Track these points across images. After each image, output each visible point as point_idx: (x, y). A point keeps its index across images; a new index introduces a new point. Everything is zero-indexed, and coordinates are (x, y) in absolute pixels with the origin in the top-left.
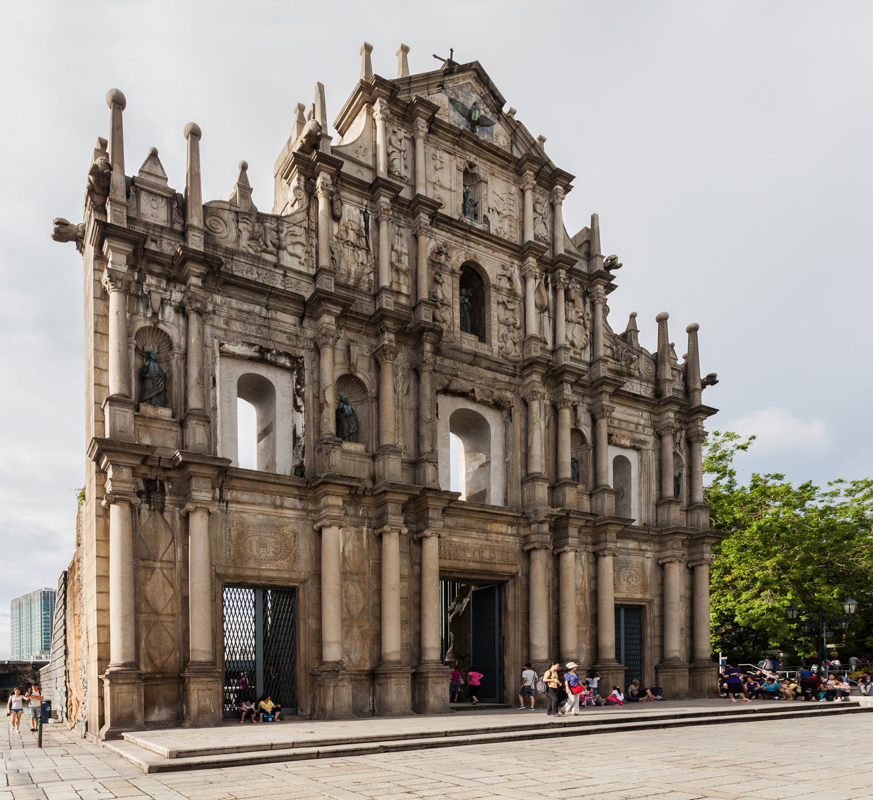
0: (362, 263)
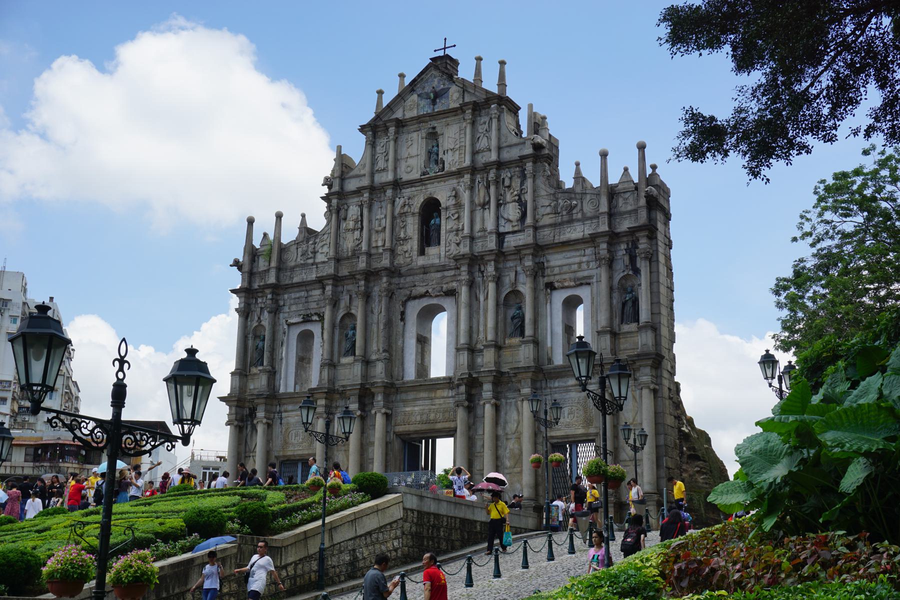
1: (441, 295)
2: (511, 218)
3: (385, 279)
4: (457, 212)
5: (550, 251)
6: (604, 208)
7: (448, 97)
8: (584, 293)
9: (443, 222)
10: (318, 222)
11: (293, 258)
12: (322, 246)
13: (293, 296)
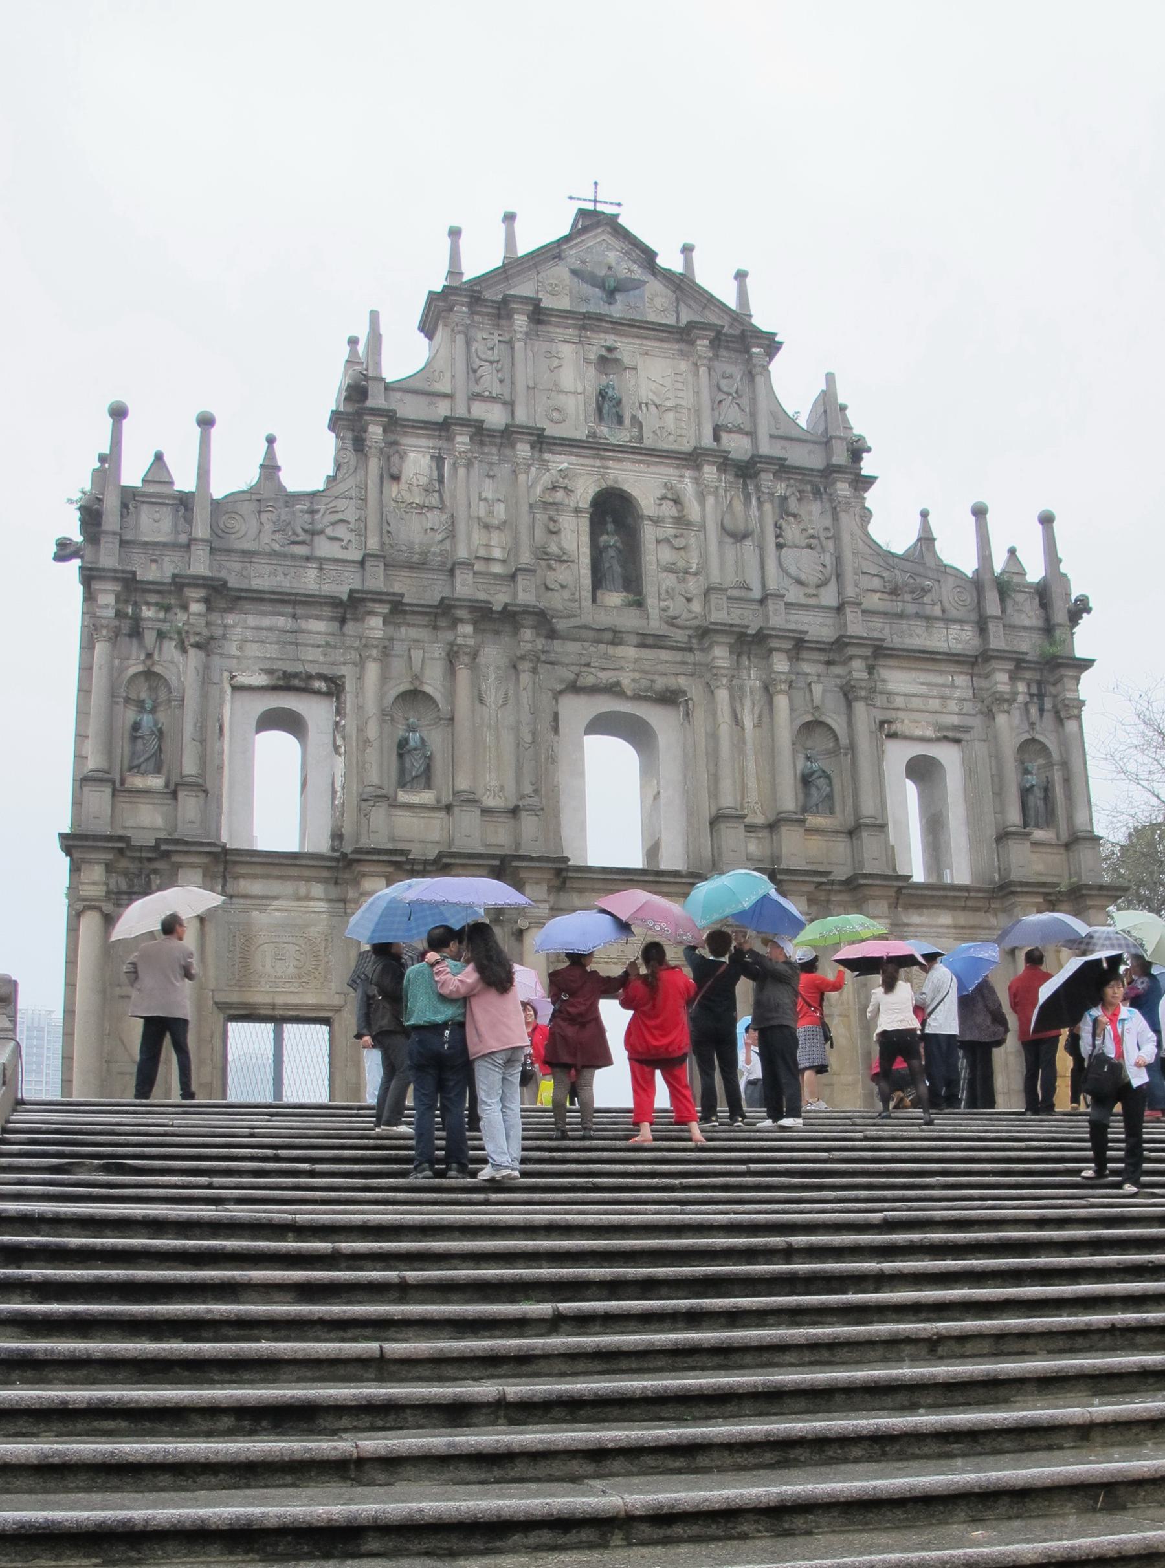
0: (432, 529)
1: (646, 699)
2: (803, 577)
4: (682, 535)
5: (890, 662)
8: (948, 756)
12: (333, 524)
13: (252, 620)
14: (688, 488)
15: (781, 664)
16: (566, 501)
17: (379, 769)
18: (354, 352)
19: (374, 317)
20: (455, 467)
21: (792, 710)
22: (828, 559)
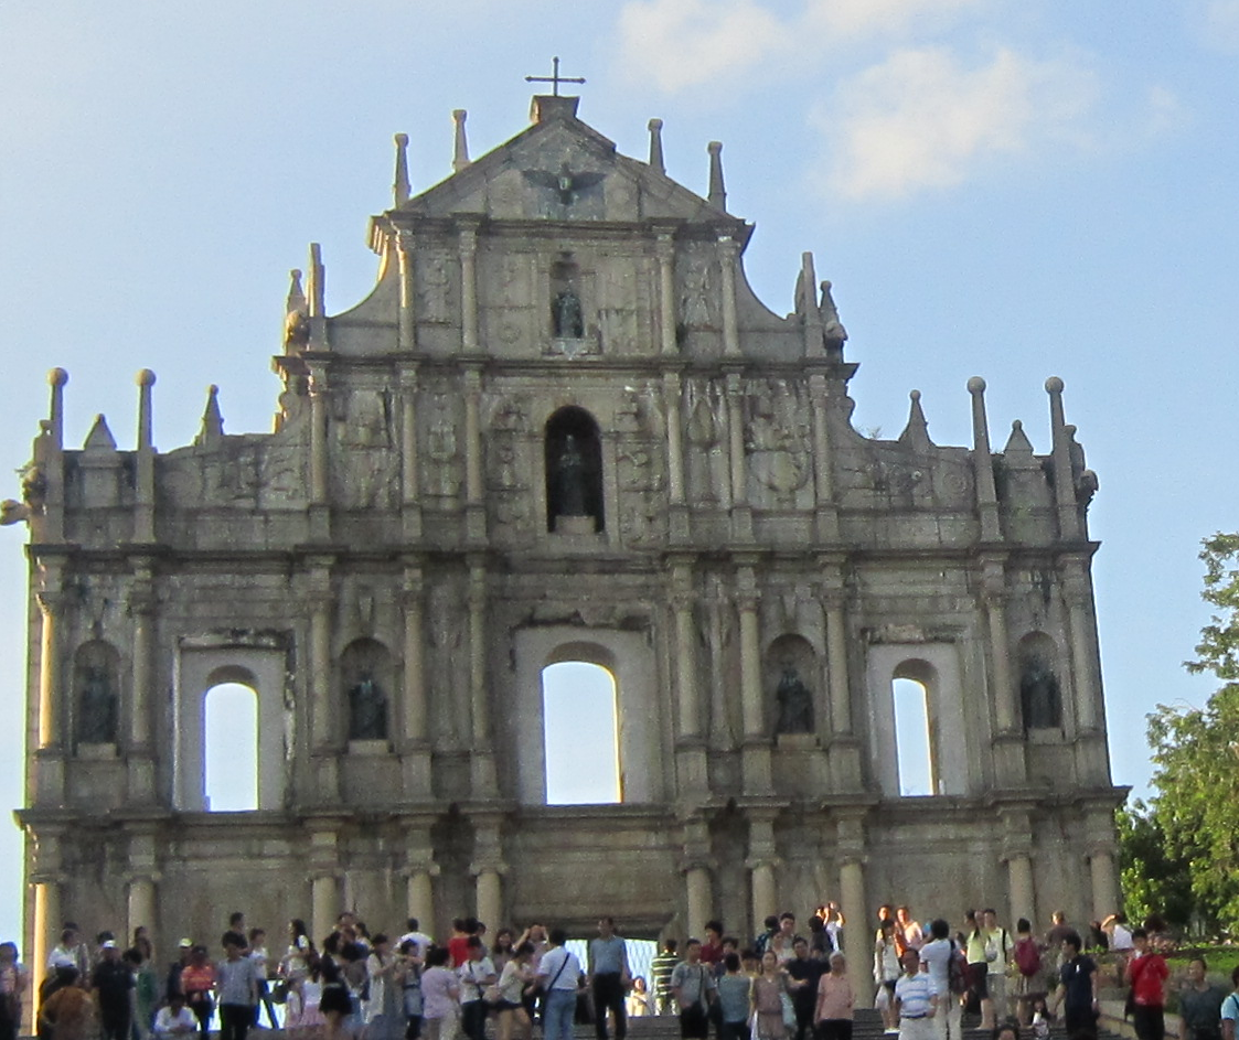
0: (379, 470)
2: (777, 482)
3: (477, 573)
5: (873, 564)
6: (988, 493)
7: (601, 195)
8: (940, 656)
9: (608, 465)
10: (256, 408)
11: (191, 489)
13: (197, 580)
14: (651, 398)
15: (747, 581)
16: (519, 428)
17: (322, 723)
18: (296, 288)
19: (316, 251)
20: (400, 402)
21: (761, 625)
22: (803, 458)
